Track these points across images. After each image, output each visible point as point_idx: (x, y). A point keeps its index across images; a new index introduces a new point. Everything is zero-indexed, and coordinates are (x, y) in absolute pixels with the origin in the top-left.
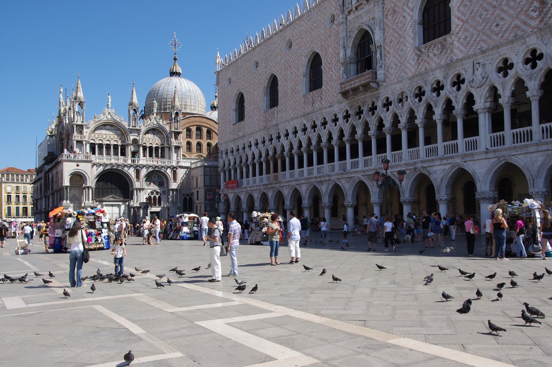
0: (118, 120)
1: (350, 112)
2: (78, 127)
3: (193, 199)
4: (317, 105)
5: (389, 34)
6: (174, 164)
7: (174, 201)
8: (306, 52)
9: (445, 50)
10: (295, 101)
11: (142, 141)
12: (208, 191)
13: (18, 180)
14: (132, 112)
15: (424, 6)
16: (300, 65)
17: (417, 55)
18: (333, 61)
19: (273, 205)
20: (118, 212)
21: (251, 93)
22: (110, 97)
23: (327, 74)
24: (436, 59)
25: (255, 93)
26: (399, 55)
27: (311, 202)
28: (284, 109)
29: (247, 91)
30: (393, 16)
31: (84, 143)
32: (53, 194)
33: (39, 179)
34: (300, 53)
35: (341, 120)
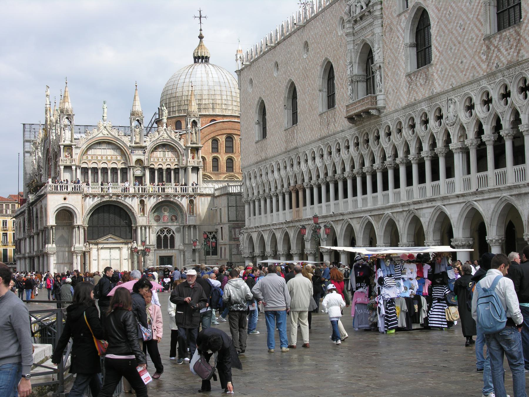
2: (66, 148)
4: (331, 128)
11: (149, 161)
12: (234, 228)
15: (416, 26)
17: (408, 82)
18: (344, 76)
20: (118, 257)
23: (339, 91)
25: (276, 104)
26: (395, 79)
29: (268, 100)
30: (390, 34)
31: (74, 168)
32: (38, 234)
33: (22, 213)
34: (315, 61)
35: (352, 148)
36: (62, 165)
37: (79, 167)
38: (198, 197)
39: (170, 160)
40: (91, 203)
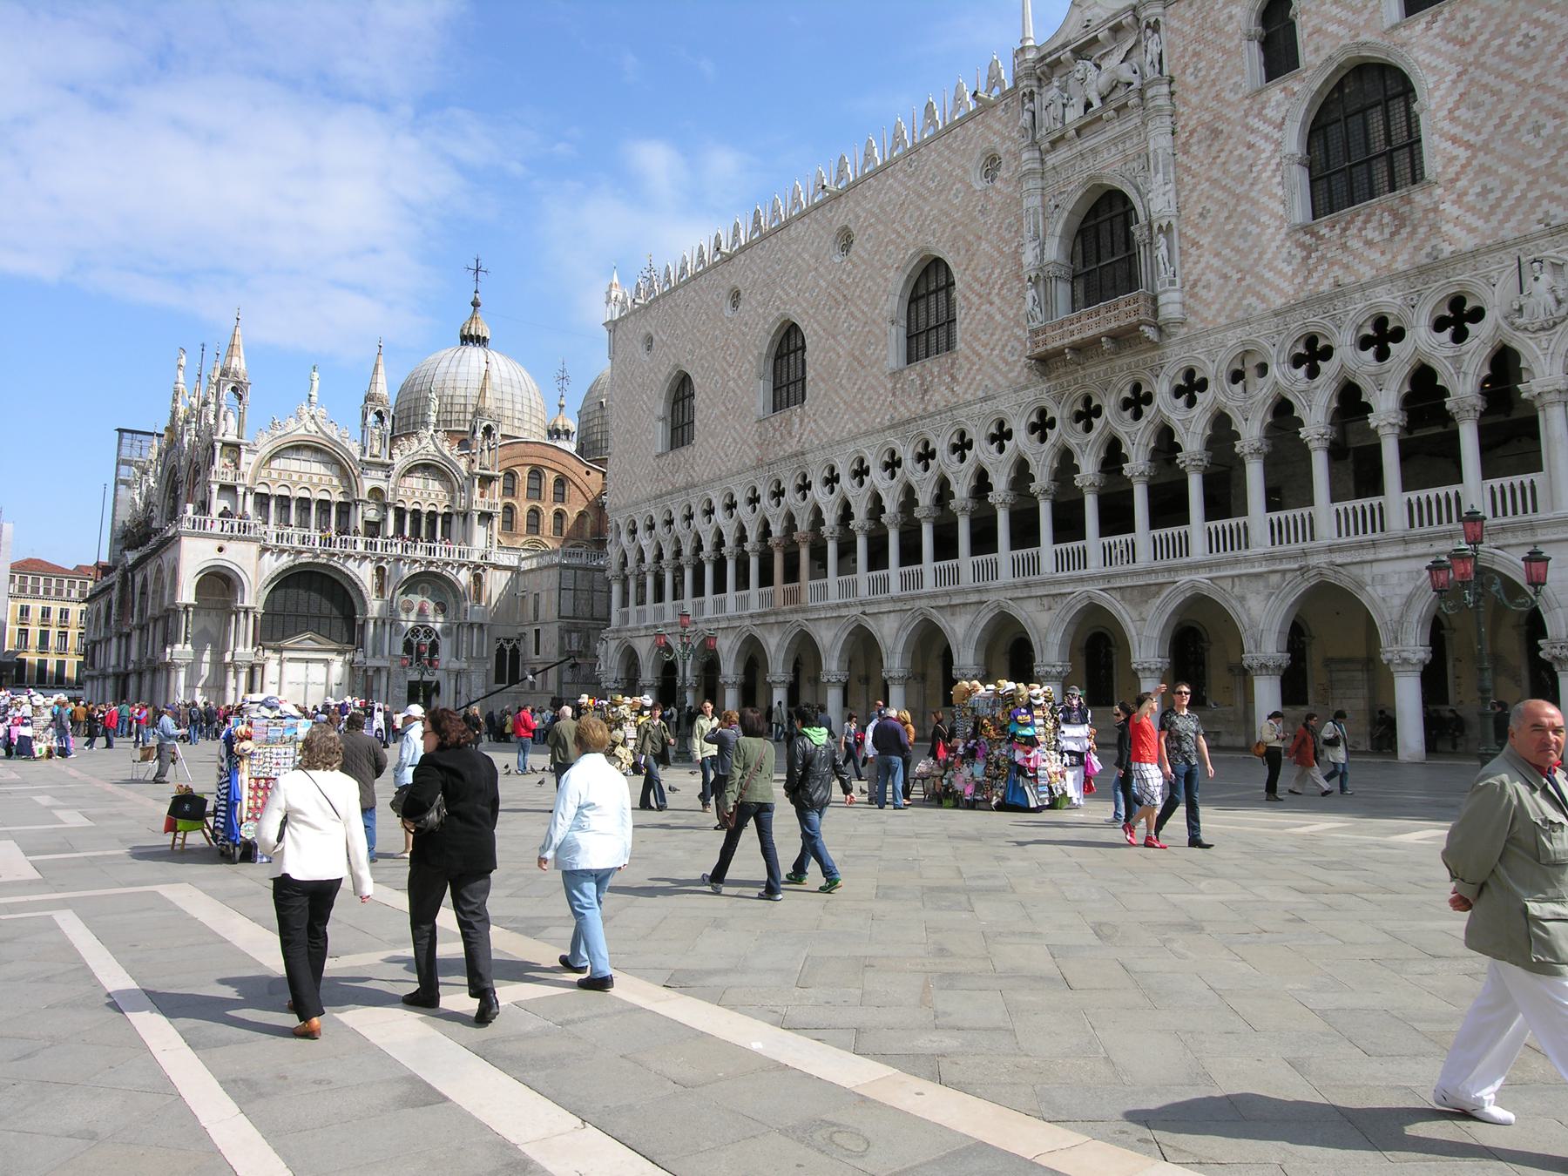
0: (335, 437)
1: (1053, 412)
2: (227, 449)
3: (521, 651)
4: (937, 397)
5: (1195, 194)
6: (475, 558)
7: (474, 655)
8: (901, 256)
9: (1408, 229)
10: (864, 388)
12: (569, 632)
13: (47, 591)
14: (372, 418)
15: (1312, 117)
16: (880, 293)
19: (781, 671)
20: (324, 680)
21: (716, 371)
22: (316, 375)
23: (973, 311)
24: (1374, 255)
25: (730, 372)
26: (1236, 250)
27: (908, 664)
28: (823, 412)
29: (702, 367)
31: (241, 490)
32: (142, 628)
33: (107, 589)
36: (215, 482)
37: (251, 490)
38: (490, 570)
39: (437, 495)
40: (274, 565)
